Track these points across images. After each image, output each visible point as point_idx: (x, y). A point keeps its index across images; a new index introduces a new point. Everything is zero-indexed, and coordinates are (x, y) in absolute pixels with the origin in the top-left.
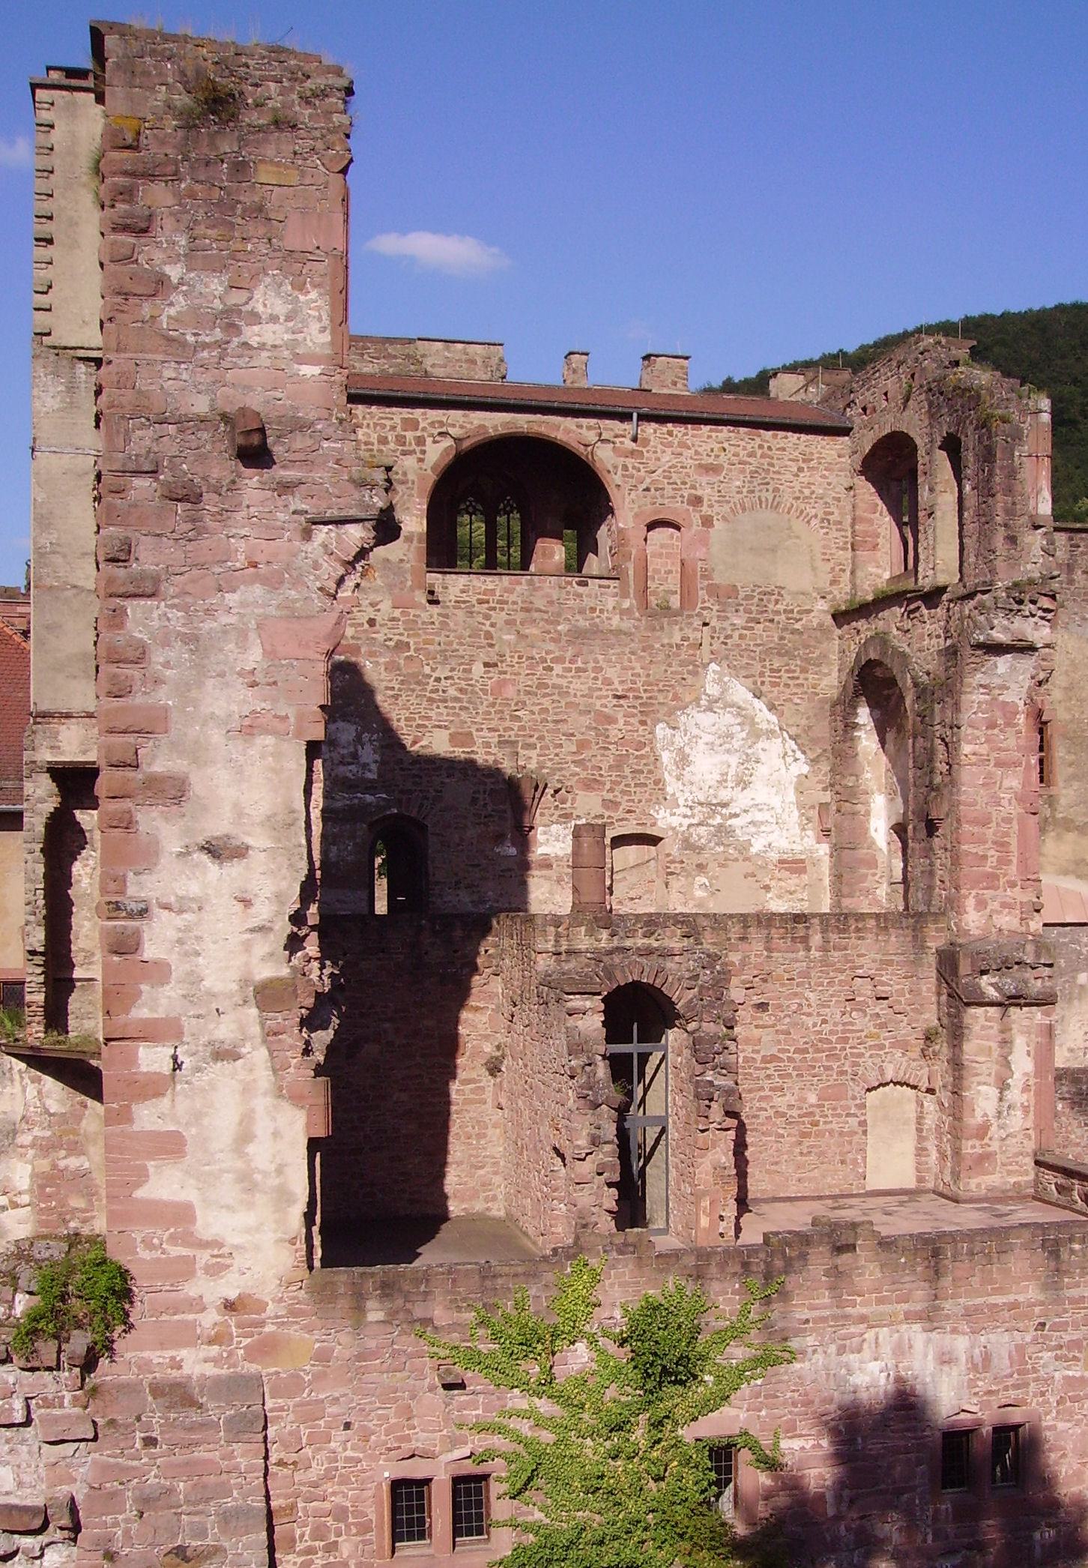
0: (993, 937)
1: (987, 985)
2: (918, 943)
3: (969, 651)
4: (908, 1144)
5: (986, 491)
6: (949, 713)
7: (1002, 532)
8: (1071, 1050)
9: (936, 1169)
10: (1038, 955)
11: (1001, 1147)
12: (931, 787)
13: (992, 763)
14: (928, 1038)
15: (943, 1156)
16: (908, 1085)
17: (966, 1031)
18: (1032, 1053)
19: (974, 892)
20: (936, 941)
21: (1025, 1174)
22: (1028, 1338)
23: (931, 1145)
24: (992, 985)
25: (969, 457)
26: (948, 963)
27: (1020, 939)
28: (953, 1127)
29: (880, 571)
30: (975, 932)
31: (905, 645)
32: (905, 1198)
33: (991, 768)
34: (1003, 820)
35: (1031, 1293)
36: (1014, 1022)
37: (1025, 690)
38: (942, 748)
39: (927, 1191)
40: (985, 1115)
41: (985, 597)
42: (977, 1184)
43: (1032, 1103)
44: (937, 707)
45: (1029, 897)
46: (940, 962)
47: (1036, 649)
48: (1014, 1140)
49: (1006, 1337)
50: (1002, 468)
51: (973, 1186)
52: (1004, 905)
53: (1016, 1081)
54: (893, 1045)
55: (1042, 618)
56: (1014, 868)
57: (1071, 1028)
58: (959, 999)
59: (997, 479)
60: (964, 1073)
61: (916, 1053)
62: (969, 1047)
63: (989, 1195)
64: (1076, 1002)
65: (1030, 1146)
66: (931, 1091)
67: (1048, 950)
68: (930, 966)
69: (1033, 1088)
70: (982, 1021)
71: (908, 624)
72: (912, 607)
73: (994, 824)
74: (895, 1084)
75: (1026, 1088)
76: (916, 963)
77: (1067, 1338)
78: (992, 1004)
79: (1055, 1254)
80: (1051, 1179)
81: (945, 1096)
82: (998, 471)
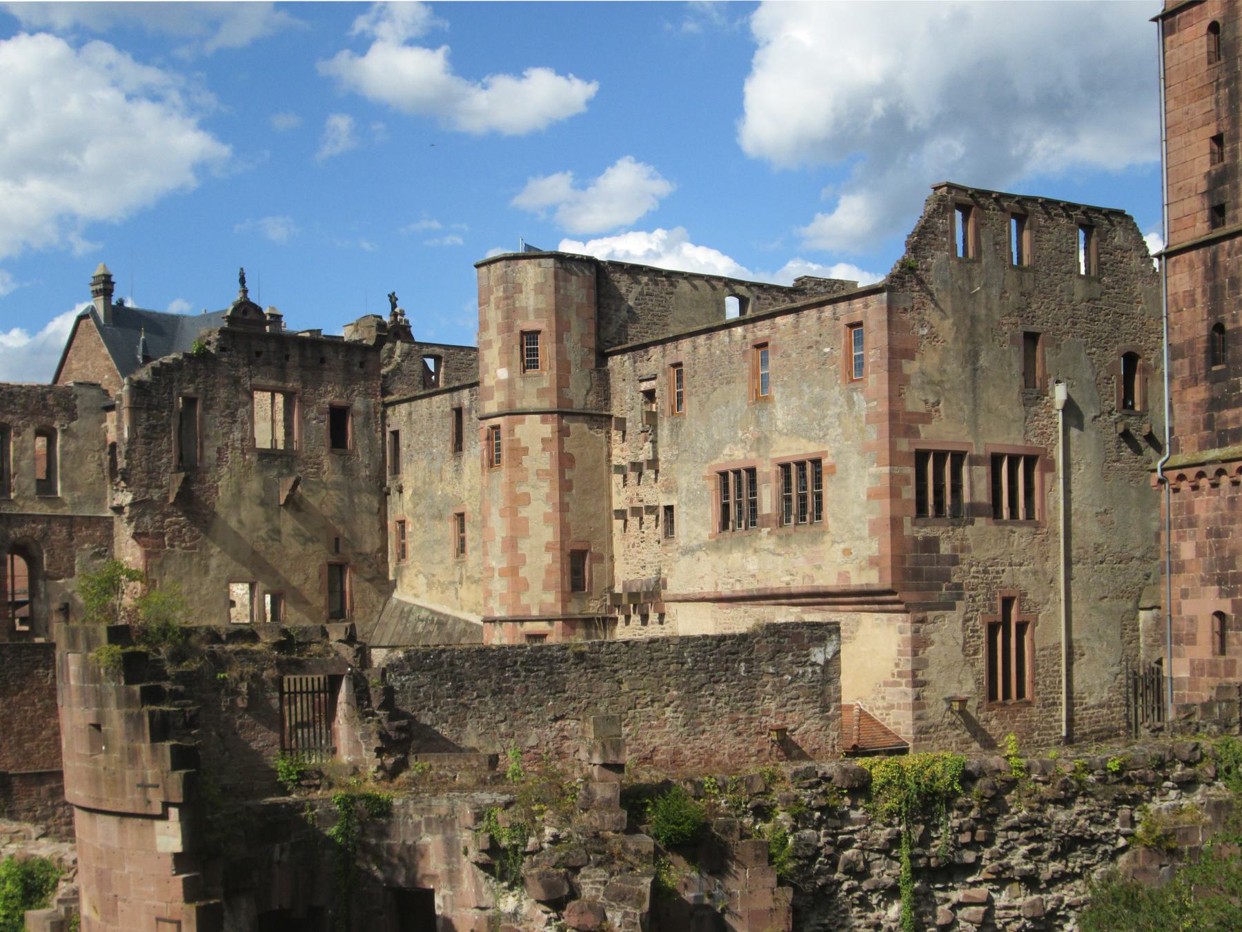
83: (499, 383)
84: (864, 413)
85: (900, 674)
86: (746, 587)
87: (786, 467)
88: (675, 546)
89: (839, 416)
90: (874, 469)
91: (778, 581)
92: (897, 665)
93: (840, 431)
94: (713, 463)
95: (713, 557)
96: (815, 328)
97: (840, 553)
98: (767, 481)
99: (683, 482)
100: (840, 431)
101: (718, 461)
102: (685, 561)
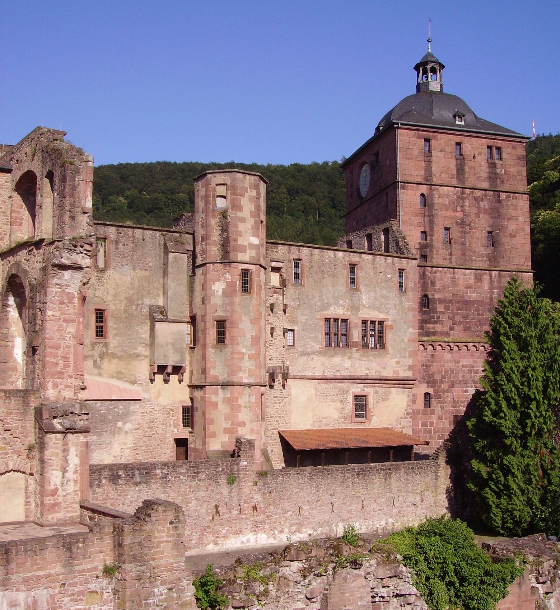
0: (61, 401)
1: (57, 424)
2: (26, 404)
3: (51, 268)
4: (21, 500)
5: (62, 196)
6: (42, 297)
7: (68, 214)
8: (115, 457)
9: (34, 512)
10: (81, 409)
11: (63, 500)
12: (35, 331)
13: (62, 320)
14: (30, 449)
15: (37, 505)
16: (21, 472)
17: (46, 445)
18: (78, 455)
19: (52, 380)
20: (34, 403)
21: (76, 512)
22: (57, 591)
23: (32, 500)
24: (59, 423)
25: (57, 180)
26: (39, 412)
27: (72, 402)
28: (40, 491)
29: (23, 235)
30: (53, 399)
31: (27, 267)
32: (18, 526)
33: (61, 322)
34: (66, 347)
35: (58, 569)
36: (70, 441)
37: (78, 287)
38: (40, 313)
39: (30, 522)
40: (56, 485)
41: (59, 243)
42: (52, 517)
43: (79, 479)
44: (38, 294)
45: (78, 382)
46: (36, 413)
47: (82, 268)
48: (70, 496)
49: (45, 591)
50: (69, 185)
51: (50, 519)
52: (66, 386)
53: (71, 468)
54: (12, 453)
55: (86, 254)
56: (72, 369)
57: (115, 446)
58: (44, 430)
59: (67, 190)
60: (45, 465)
61: (24, 456)
62: (48, 453)
63: (58, 523)
64: (117, 435)
65: (78, 499)
66: (31, 474)
67: (86, 407)
68: (31, 415)
69: (79, 472)
70: (54, 440)
71: (28, 257)
72: (30, 249)
73: (62, 349)
74: (14, 471)
75: (76, 472)
76: (24, 413)
77: (76, 590)
78: (59, 432)
79: (70, 549)
80: (87, 514)
81: (37, 476)
82: (67, 186)
83: (251, 246)
84: (407, 306)
85: (408, 414)
86: (342, 374)
87: (364, 322)
88: (295, 351)
89: (395, 305)
90: (411, 330)
91: (362, 372)
92: (406, 410)
93: (395, 311)
94: (324, 313)
95: (323, 359)
96: (384, 265)
97: (394, 363)
98: (356, 326)
99: (302, 319)
100: (395, 311)
101: (326, 312)
102: (303, 359)
